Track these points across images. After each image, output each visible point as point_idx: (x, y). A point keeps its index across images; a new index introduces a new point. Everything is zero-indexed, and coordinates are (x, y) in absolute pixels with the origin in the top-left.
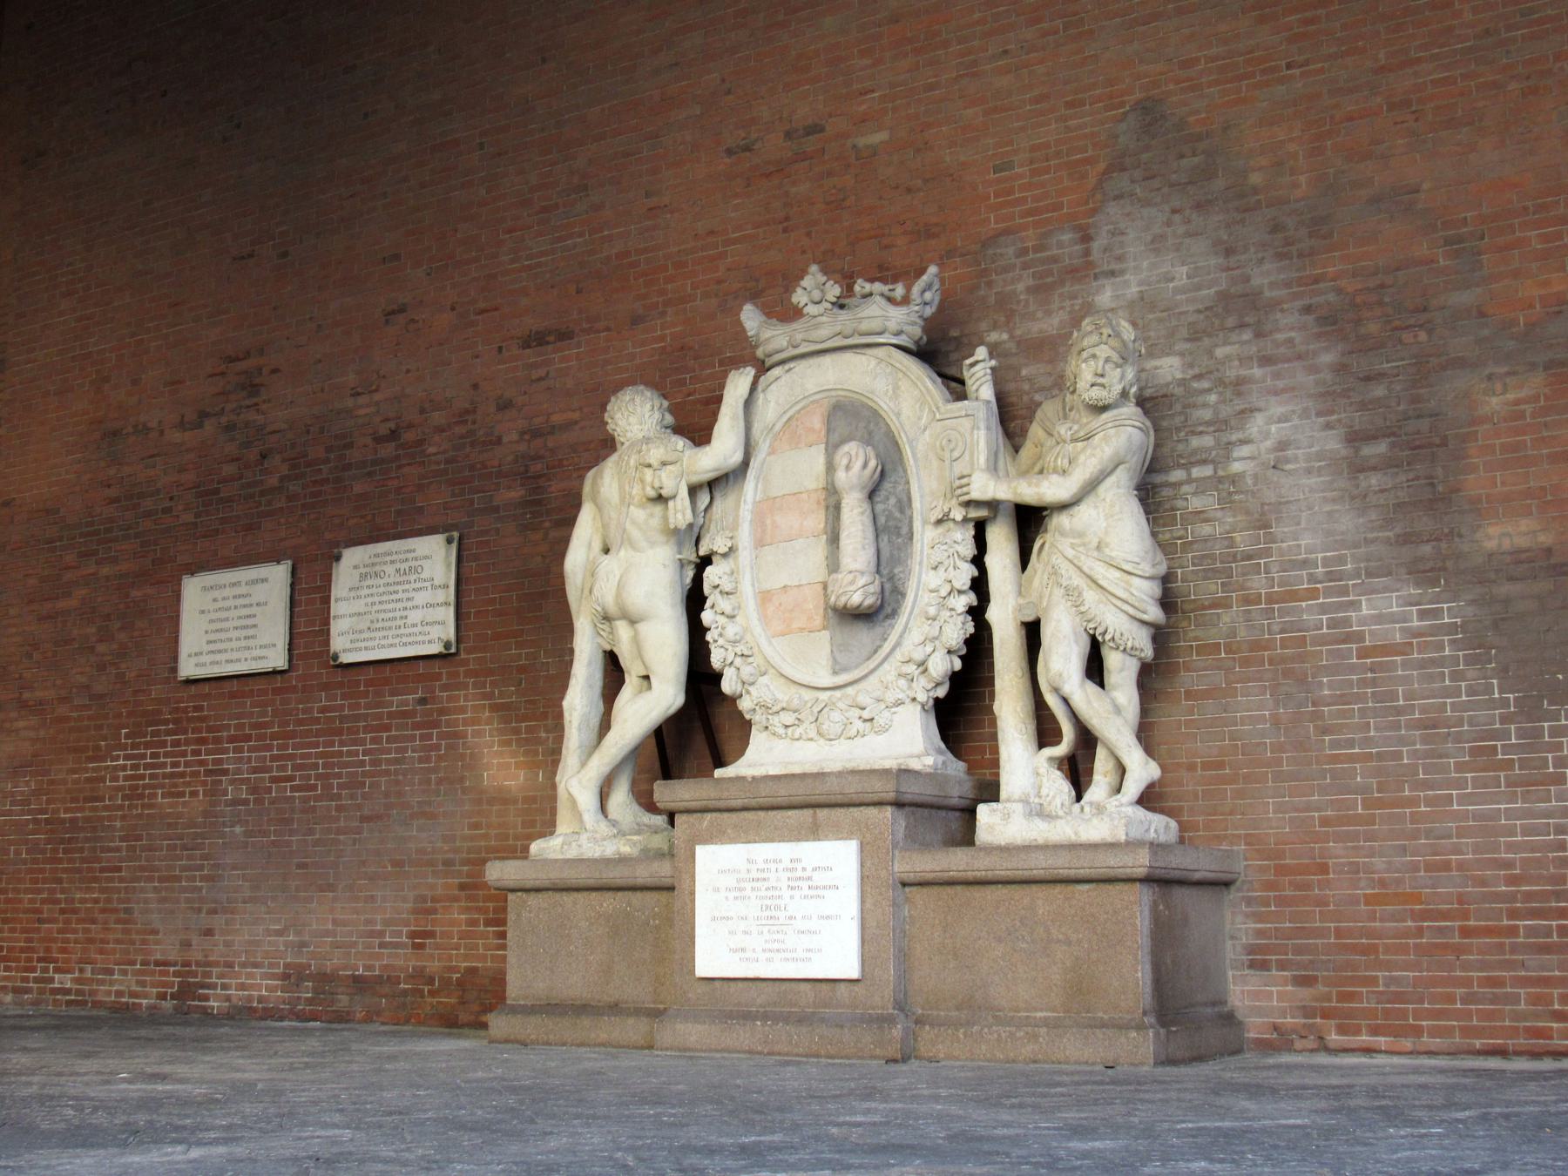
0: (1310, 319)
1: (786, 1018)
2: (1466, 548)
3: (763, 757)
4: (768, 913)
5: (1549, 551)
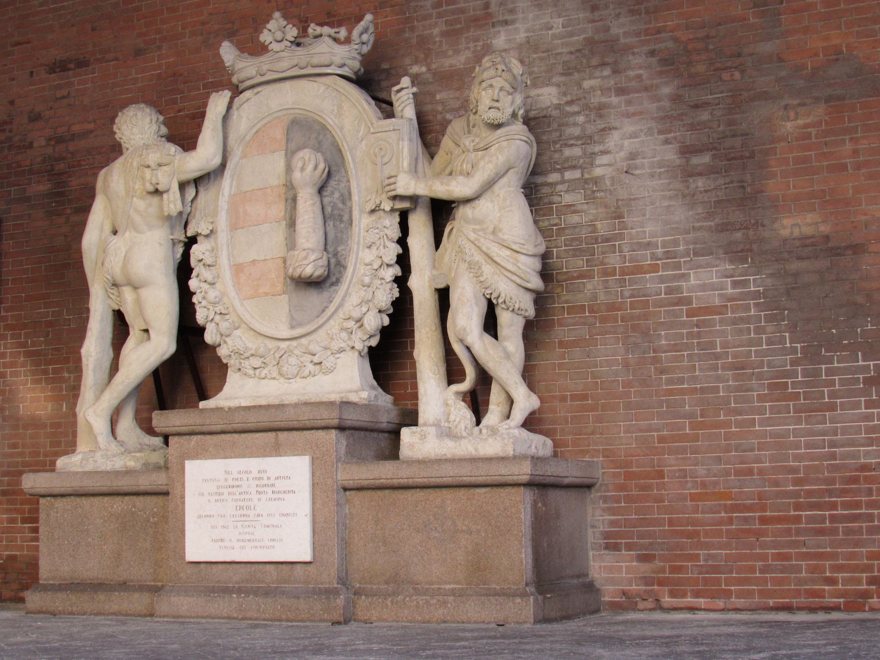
0: (654, 60)
1: (256, 592)
2: (767, 234)
3: (237, 392)
4: (239, 512)
5: (827, 238)
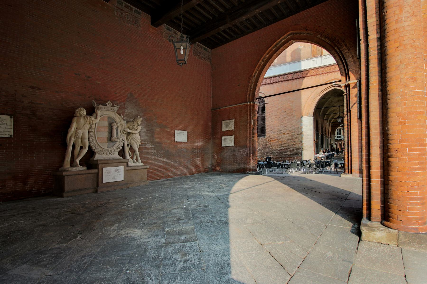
3: (97, 157)
